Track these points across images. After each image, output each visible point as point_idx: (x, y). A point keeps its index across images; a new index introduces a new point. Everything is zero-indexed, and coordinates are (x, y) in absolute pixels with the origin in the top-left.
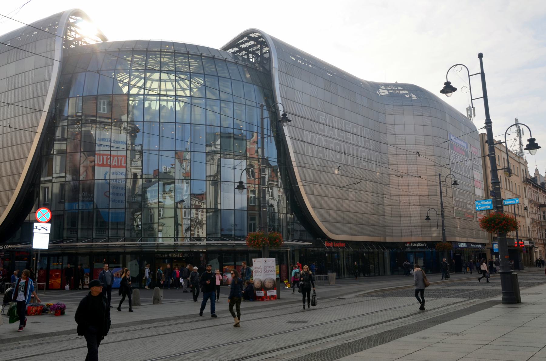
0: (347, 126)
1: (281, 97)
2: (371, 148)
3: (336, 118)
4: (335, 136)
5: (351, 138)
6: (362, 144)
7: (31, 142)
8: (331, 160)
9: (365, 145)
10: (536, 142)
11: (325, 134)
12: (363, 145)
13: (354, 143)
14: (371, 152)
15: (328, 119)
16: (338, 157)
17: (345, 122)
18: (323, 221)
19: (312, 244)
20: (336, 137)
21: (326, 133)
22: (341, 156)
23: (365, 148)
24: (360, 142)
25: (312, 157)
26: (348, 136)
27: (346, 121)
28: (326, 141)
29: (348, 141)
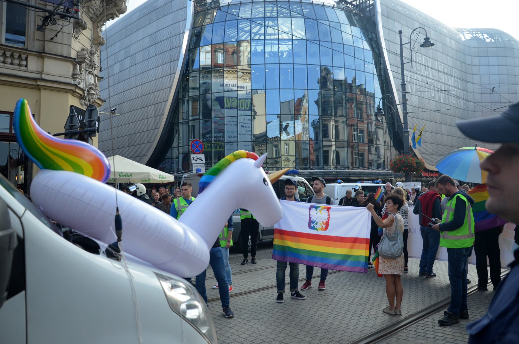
0: (439, 67)
1: (384, 39)
2: (459, 87)
3: (430, 59)
4: (430, 75)
5: (443, 77)
6: (451, 83)
7: (170, 87)
8: (427, 98)
9: (454, 84)
11: (421, 74)
12: (453, 84)
13: (445, 82)
14: (460, 91)
15: (423, 60)
16: (433, 95)
17: (438, 63)
18: (421, 153)
20: (431, 76)
21: (422, 73)
22: (435, 94)
23: (454, 87)
24: (450, 82)
26: (440, 76)
27: (439, 62)
29: (440, 80)
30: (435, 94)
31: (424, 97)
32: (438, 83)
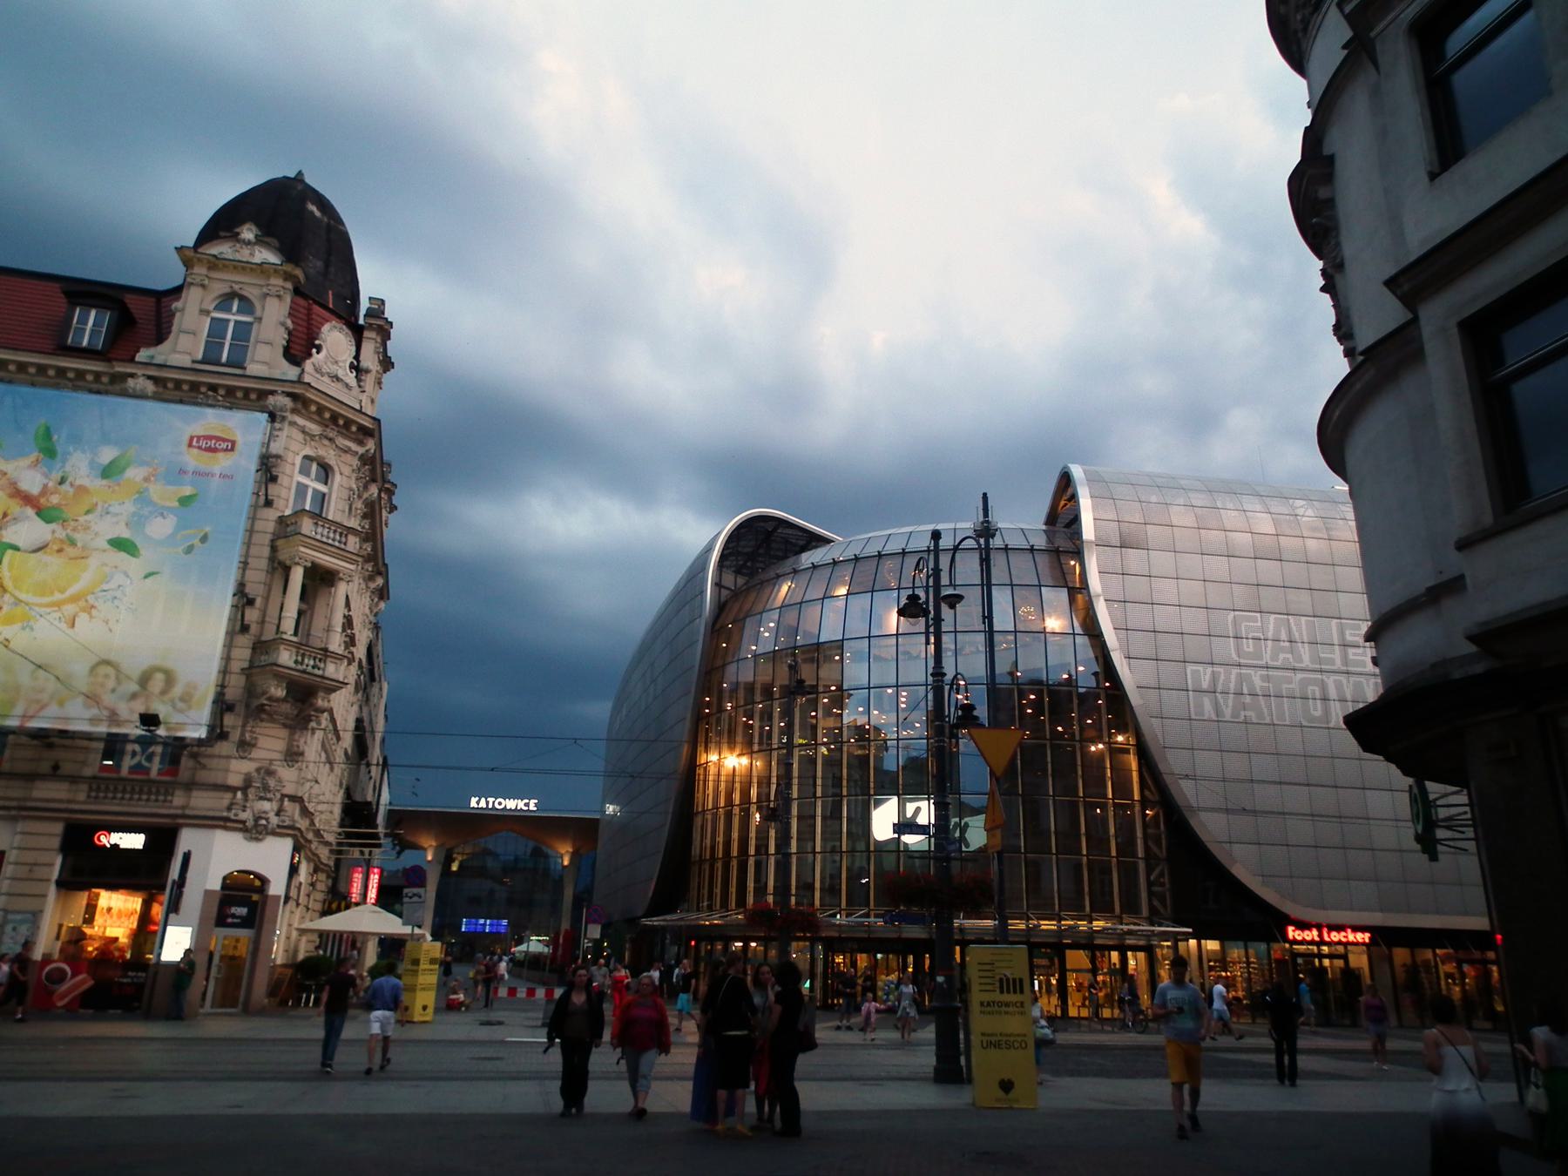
0: (1347, 632)
3: (1303, 619)
4: (1301, 661)
10: (975, 713)
19: (1190, 930)
20: (1306, 662)
21: (1267, 658)
25: (1218, 721)
26: (1351, 657)
28: (1264, 679)
30: (1327, 712)
31: (1276, 722)
32: (1342, 678)
